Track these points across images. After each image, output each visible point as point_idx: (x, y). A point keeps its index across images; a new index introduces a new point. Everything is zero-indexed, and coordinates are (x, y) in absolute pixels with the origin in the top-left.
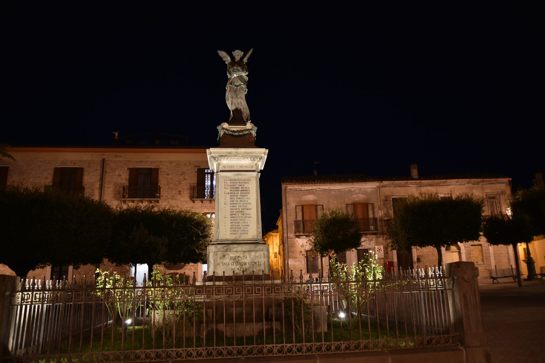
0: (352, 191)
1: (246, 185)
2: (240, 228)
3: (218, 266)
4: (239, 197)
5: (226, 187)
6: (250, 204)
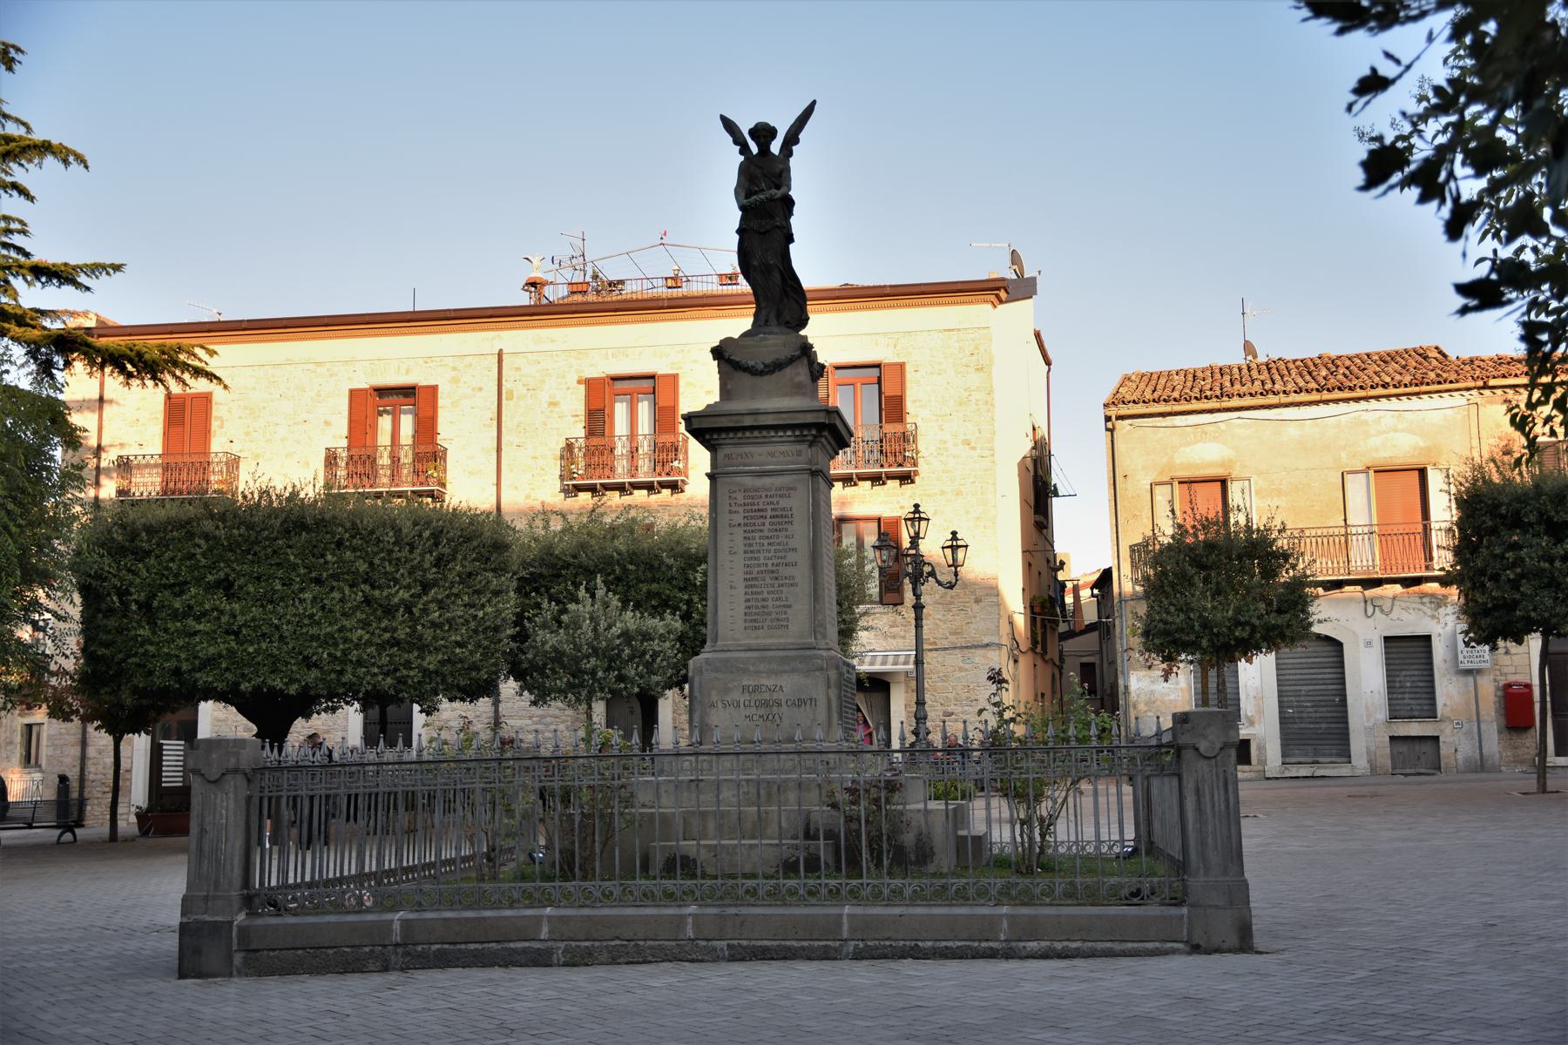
0: (1365, 423)
1: (784, 503)
2: (769, 614)
3: (713, 711)
4: (766, 533)
5: (734, 508)
6: (795, 550)
